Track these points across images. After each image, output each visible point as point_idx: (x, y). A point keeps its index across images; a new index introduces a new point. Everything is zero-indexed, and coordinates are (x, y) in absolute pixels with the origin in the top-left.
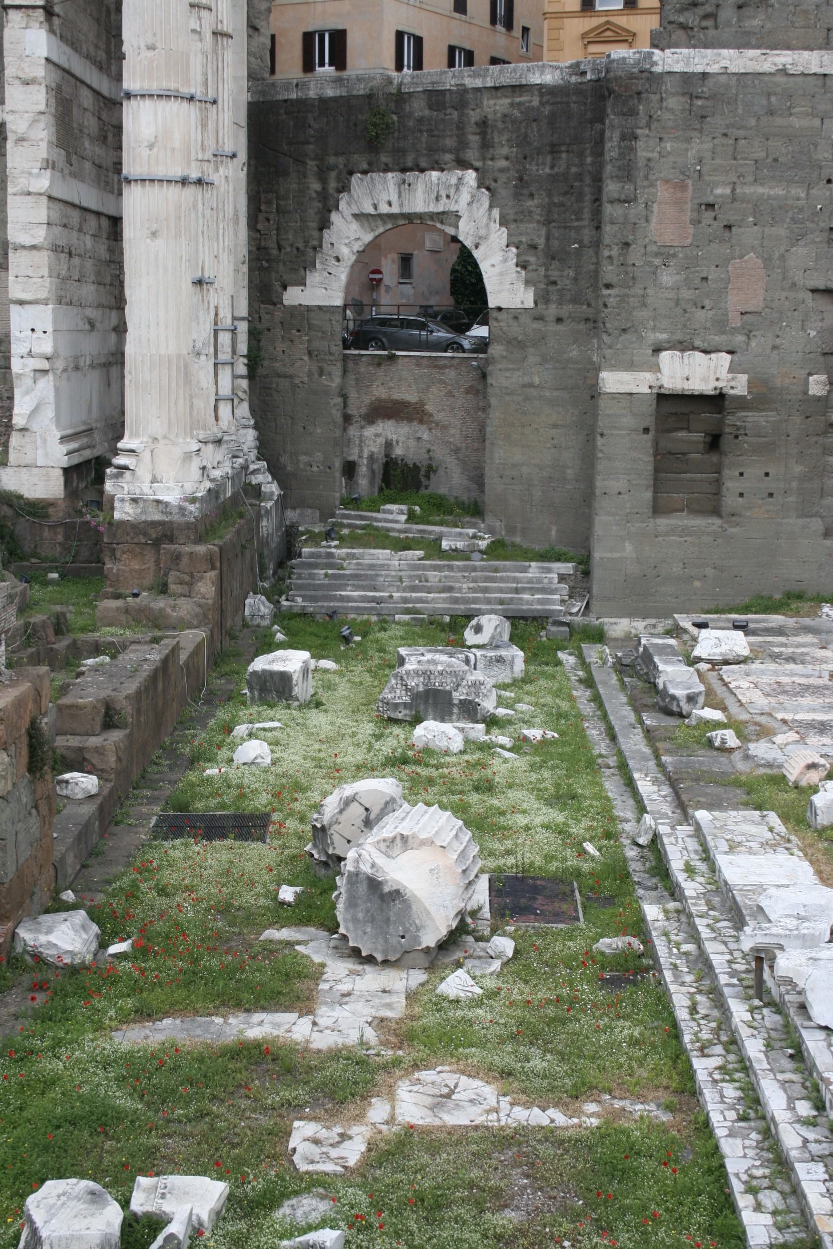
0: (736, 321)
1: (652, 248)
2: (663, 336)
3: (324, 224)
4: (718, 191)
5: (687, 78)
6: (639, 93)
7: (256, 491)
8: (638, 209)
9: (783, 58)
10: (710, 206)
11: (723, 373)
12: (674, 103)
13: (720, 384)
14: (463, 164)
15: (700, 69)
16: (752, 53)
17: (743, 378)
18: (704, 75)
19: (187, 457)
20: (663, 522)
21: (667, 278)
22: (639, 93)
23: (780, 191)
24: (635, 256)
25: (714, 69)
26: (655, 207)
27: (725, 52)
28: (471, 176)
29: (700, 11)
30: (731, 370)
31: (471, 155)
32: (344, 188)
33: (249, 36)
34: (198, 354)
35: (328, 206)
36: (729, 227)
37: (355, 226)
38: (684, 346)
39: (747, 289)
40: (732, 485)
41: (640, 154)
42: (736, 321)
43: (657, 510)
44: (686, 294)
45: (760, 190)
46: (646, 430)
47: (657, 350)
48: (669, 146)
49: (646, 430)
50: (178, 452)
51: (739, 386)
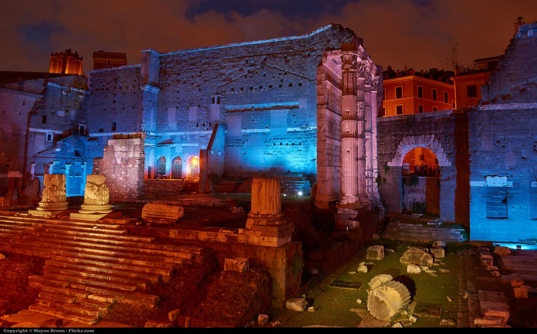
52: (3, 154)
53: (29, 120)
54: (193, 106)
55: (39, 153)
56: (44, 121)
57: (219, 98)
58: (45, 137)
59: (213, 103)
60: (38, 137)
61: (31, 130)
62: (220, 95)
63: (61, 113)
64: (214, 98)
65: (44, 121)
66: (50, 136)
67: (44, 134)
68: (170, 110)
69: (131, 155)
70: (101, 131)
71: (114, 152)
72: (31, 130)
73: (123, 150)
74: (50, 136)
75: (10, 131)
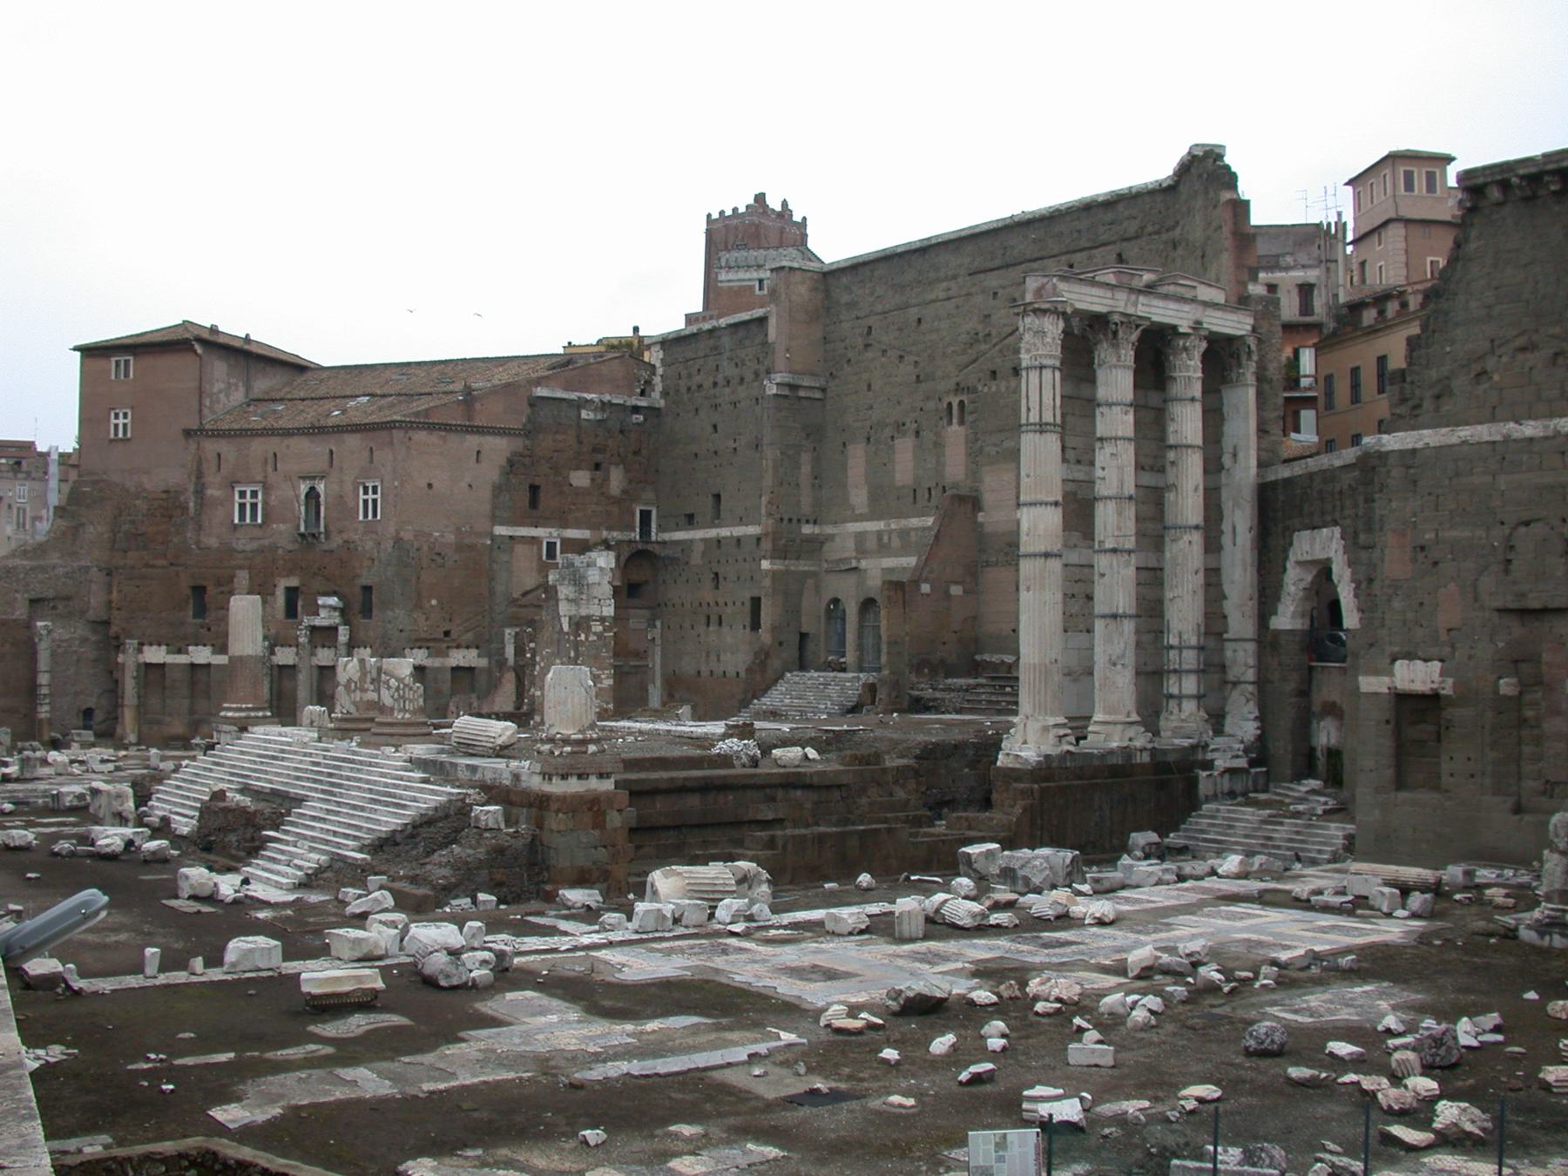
0: (1444, 637)
1: (1387, 582)
2: (1396, 649)
3: (1285, 570)
4: (1427, 536)
5: (1403, 454)
6: (1374, 468)
7: (1208, 765)
8: (1376, 553)
9: (1465, 432)
10: (1423, 548)
11: (1436, 677)
12: (1396, 473)
13: (1435, 686)
14: (1335, 523)
15: (1410, 446)
16: (1444, 430)
17: (1450, 681)
18: (1414, 451)
19: (1046, 729)
20: (1403, 795)
21: (1397, 604)
22: (1374, 468)
23: (1467, 534)
24: (1376, 586)
25: (1420, 445)
26: (1387, 551)
27: (1425, 432)
28: (1337, 530)
29: (1410, 403)
30: (1441, 675)
31: (1337, 515)
32: (1291, 544)
33: (1259, 438)
34: (1114, 665)
35: (1286, 558)
36: (1436, 563)
37: (1298, 570)
38: (1410, 656)
39: (1450, 611)
40: (1445, 767)
41: (1378, 512)
42: (1444, 637)
43: (1400, 784)
44: (1410, 616)
45: (1455, 533)
46: (1388, 722)
47: (1394, 660)
48: (1394, 505)
49: (1388, 722)
50: (1038, 725)
51: (1447, 689)
52: (434, 602)
53: (495, 507)
54: (904, 434)
55: (525, 594)
56: (534, 503)
57: (961, 402)
58: (540, 549)
59: (950, 422)
60: (519, 549)
61: (501, 530)
62: (964, 398)
63: (580, 479)
64: (950, 404)
65: (534, 503)
66: (551, 546)
67: (535, 540)
68: (850, 447)
69: (583, 612)
70: (690, 520)
71: (557, 601)
72: (501, 530)
73: (571, 596)
74: (551, 546)
75: (451, 538)
